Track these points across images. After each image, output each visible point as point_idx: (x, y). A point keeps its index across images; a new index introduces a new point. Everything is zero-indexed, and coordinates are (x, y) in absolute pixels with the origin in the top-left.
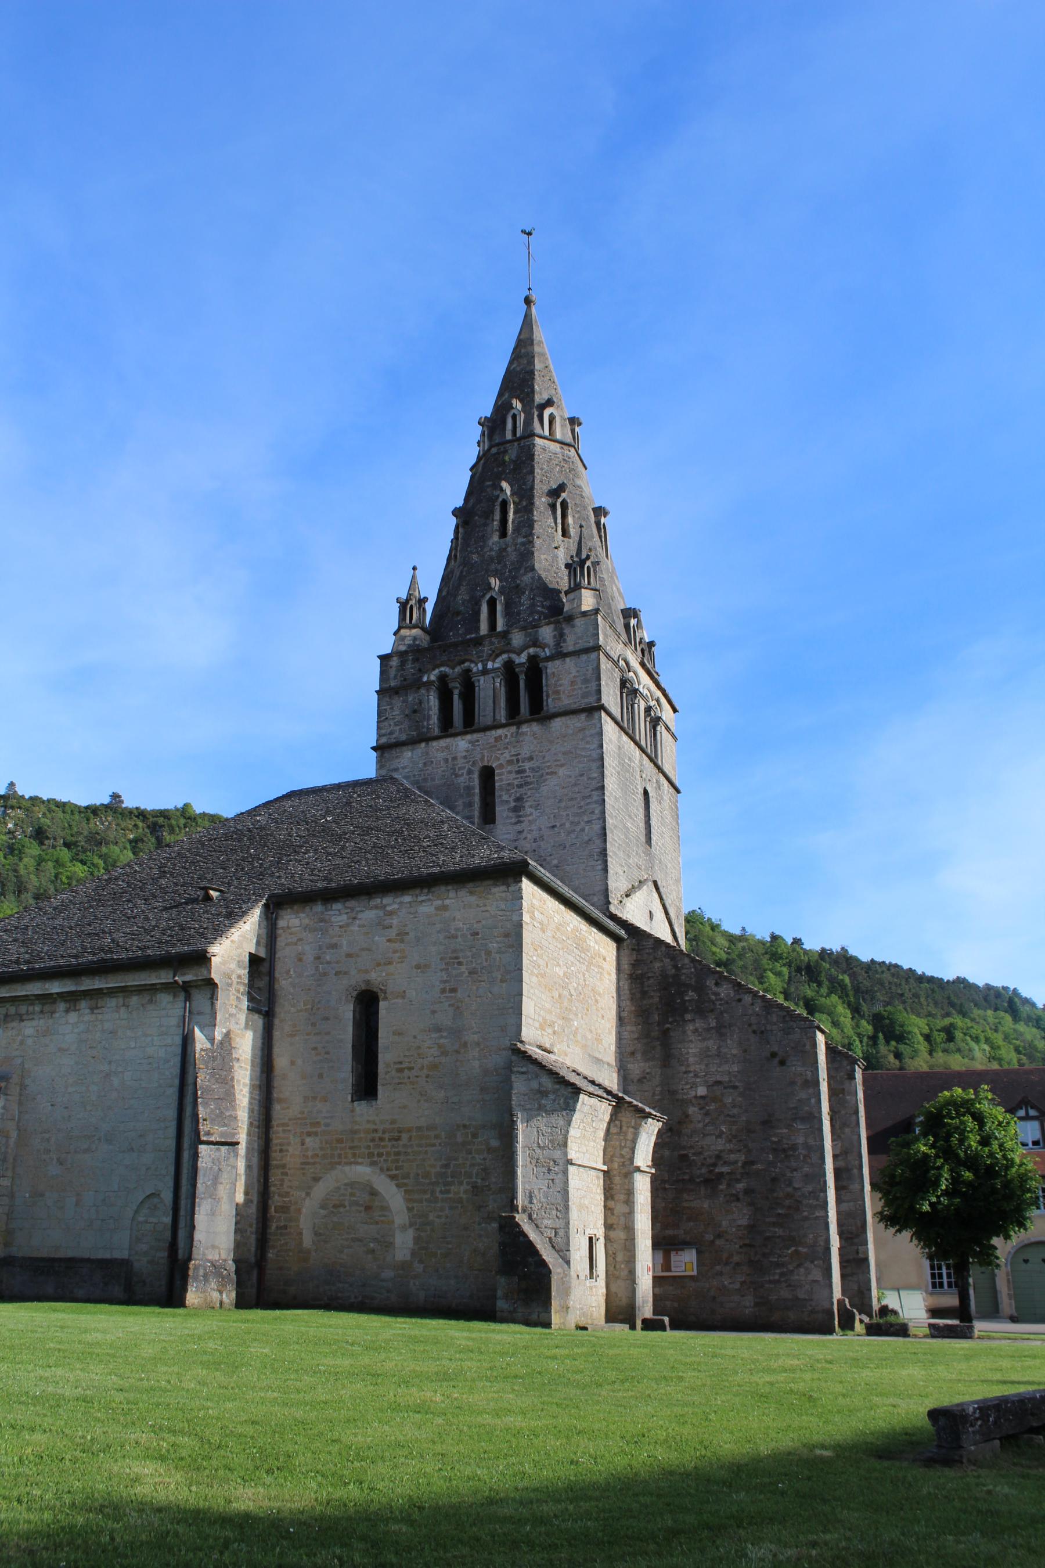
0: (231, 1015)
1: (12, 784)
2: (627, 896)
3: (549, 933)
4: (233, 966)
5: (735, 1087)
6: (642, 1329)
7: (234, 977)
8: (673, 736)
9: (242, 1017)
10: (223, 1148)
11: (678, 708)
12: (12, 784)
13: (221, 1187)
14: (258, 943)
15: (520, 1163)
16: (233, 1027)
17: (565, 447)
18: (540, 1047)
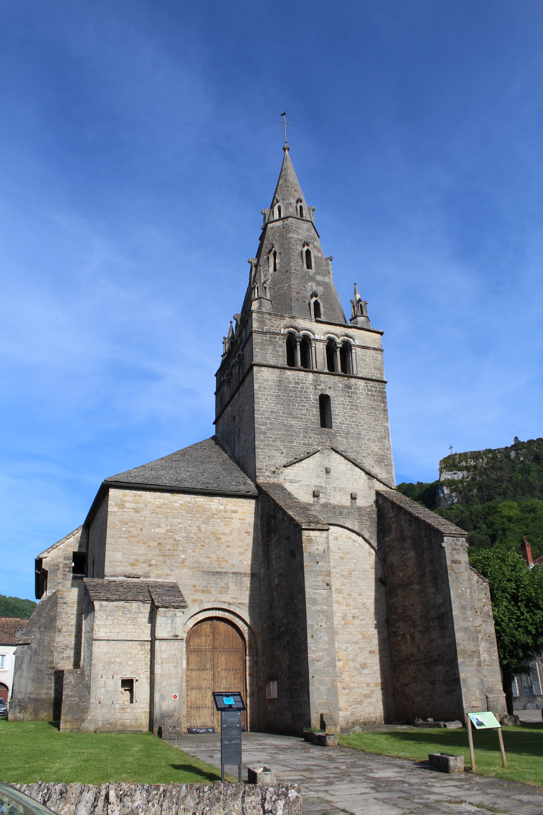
0: (58, 583)
1: (516, 438)
2: (285, 466)
3: (146, 512)
4: (61, 560)
5: (284, 576)
6: (251, 731)
7: (61, 566)
8: (374, 349)
9: (69, 583)
10: (25, 646)
11: (381, 331)
12: (516, 438)
13: (24, 664)
14: (80, 546)
15: (83, 642)
16: (60, 587)
17: (285, 220)
18: (126, 576)
